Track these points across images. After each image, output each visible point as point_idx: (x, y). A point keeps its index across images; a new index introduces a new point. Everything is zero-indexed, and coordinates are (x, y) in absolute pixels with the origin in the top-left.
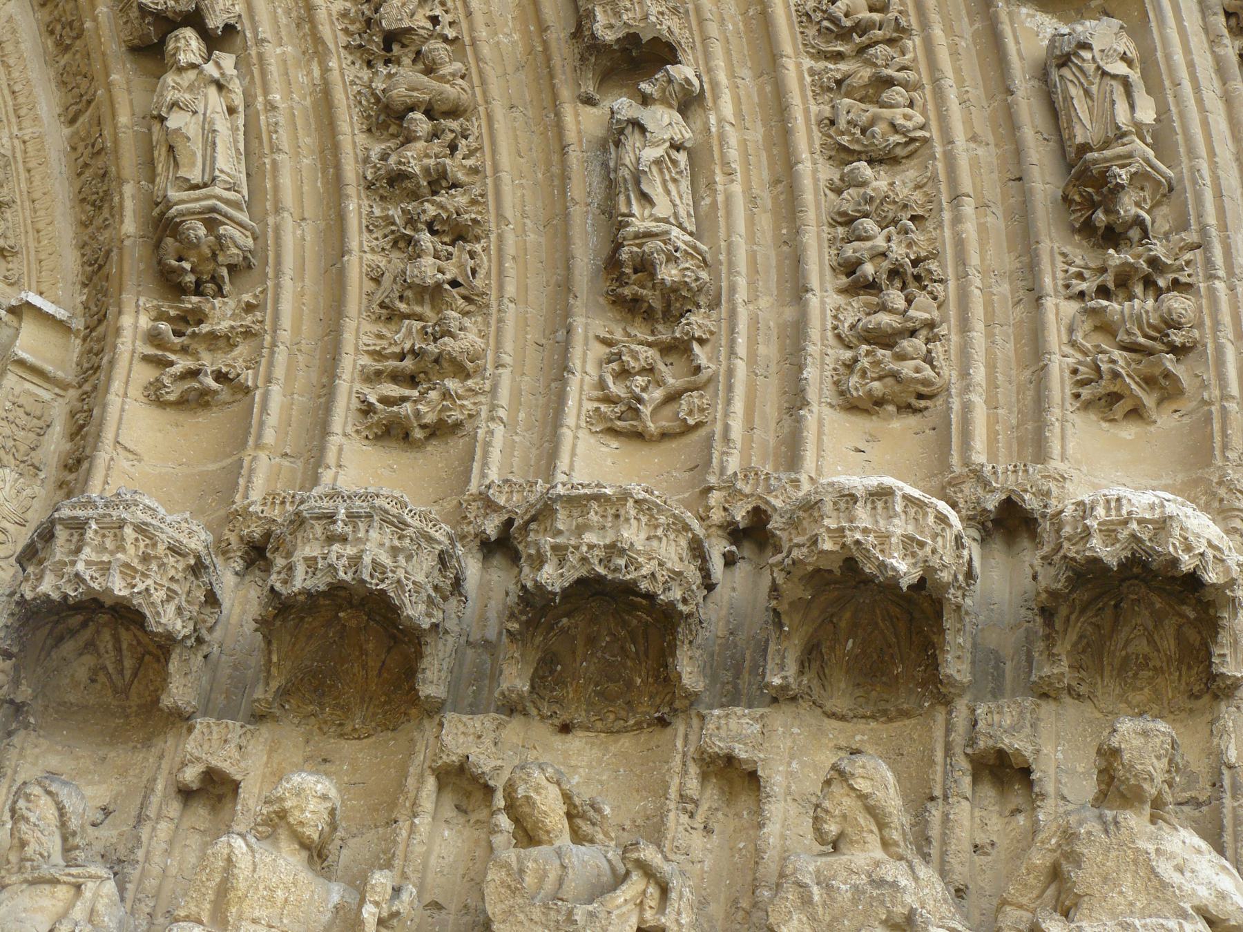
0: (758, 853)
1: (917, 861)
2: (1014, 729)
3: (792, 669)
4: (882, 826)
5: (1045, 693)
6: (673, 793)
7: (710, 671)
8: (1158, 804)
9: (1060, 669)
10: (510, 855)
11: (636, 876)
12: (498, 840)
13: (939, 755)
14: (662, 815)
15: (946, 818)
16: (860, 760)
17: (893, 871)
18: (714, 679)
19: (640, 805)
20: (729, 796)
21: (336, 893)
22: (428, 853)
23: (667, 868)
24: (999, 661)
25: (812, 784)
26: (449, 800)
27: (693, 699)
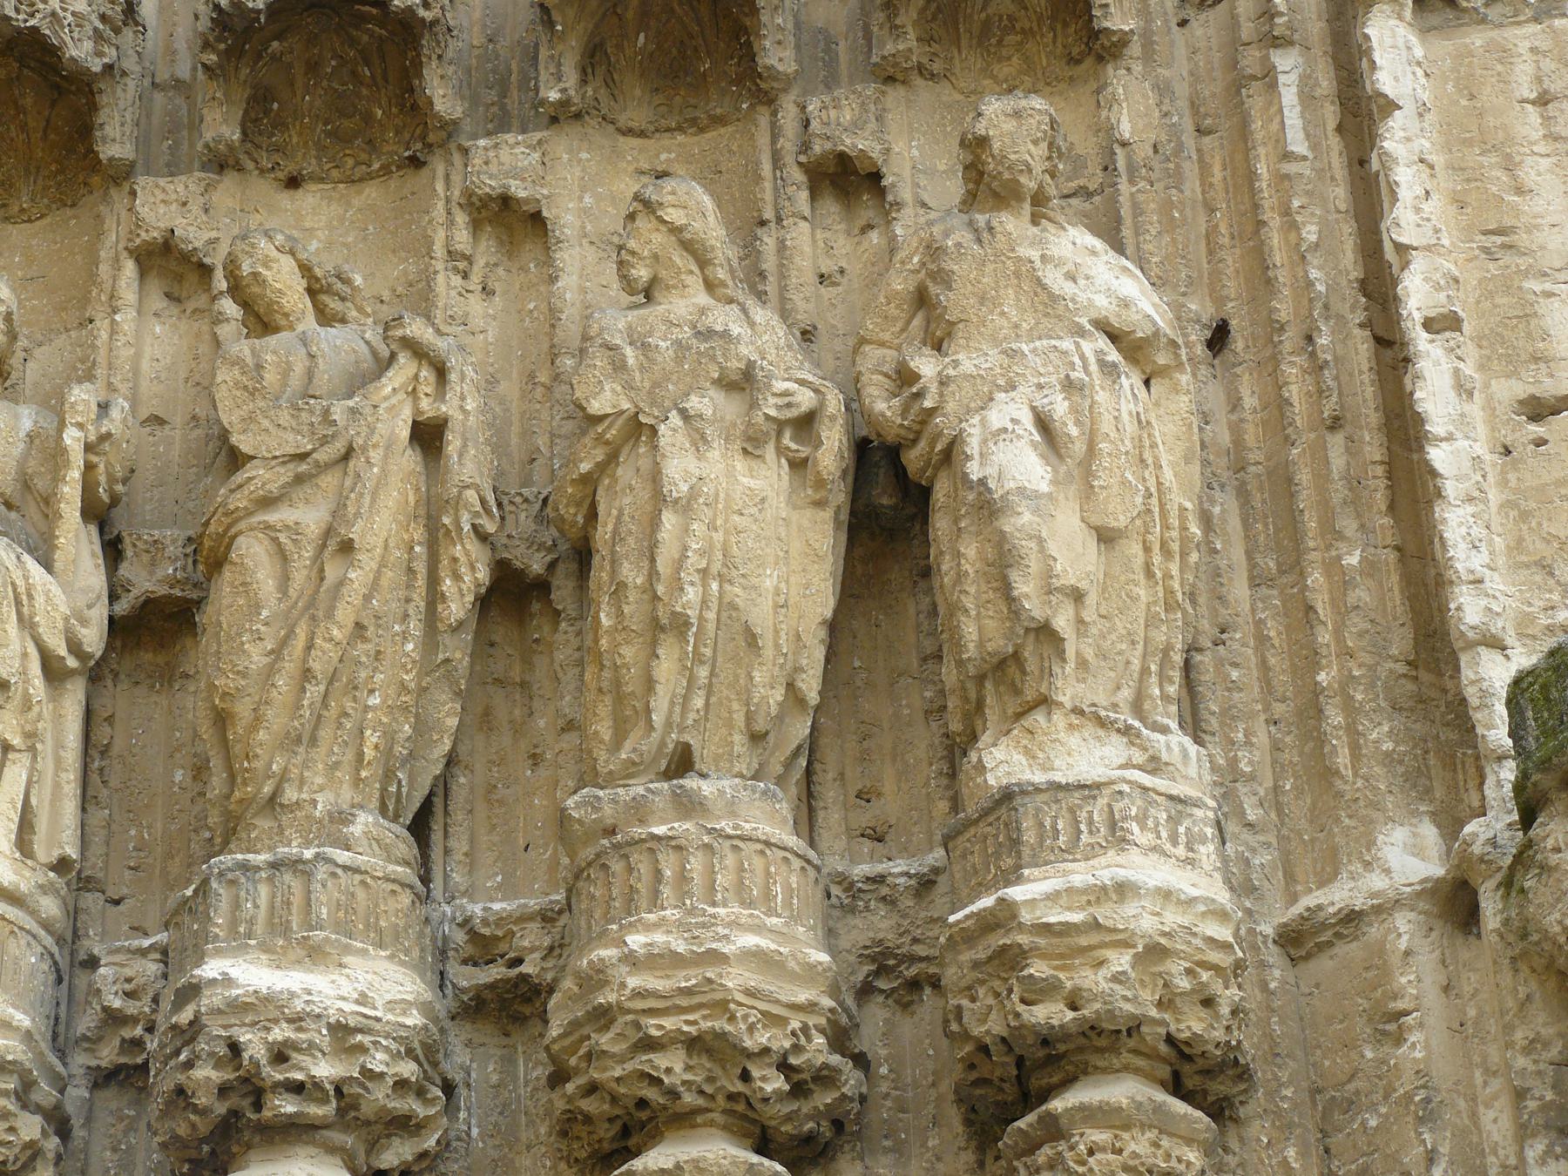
0: (553, 313)
1: (750, 303)
2: (856, 126)
3: (571, 79)
4: (703, 263)
5: (890, 76)
6: (439, 250)
7: (468, 91)
8: (1039, 199)
9: (906, 44)
10: (243, 348)
11: (403, 358)
12: (224, 331)
13: (766, 168)
14: (428, 278)
15: (782, 246)
16: (669, 184)
17: (723, 318)
18: (474, 101)
19: (397, 270)
20: (510, 246)
21: (26, 418)
22: (138, 356)
23: (442, 344)
24: (830, 42)
25: (612, 220)
26: (155, 289)
27: (450, 128)
